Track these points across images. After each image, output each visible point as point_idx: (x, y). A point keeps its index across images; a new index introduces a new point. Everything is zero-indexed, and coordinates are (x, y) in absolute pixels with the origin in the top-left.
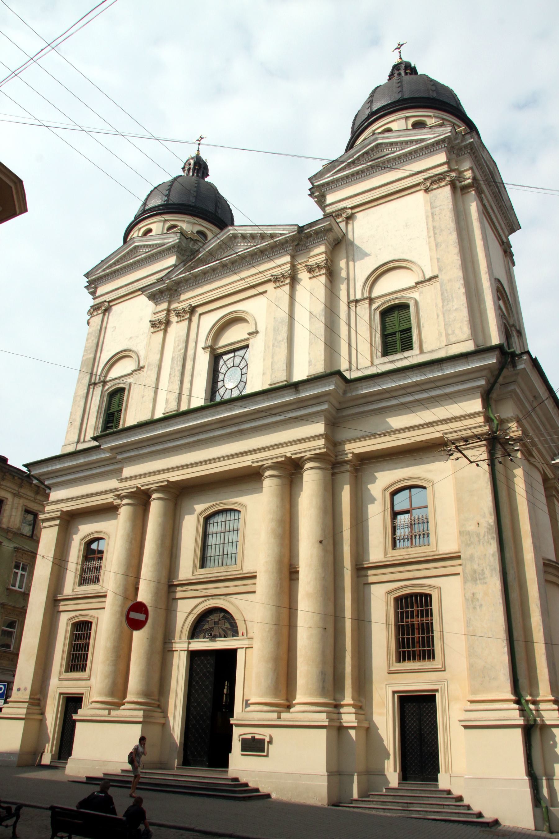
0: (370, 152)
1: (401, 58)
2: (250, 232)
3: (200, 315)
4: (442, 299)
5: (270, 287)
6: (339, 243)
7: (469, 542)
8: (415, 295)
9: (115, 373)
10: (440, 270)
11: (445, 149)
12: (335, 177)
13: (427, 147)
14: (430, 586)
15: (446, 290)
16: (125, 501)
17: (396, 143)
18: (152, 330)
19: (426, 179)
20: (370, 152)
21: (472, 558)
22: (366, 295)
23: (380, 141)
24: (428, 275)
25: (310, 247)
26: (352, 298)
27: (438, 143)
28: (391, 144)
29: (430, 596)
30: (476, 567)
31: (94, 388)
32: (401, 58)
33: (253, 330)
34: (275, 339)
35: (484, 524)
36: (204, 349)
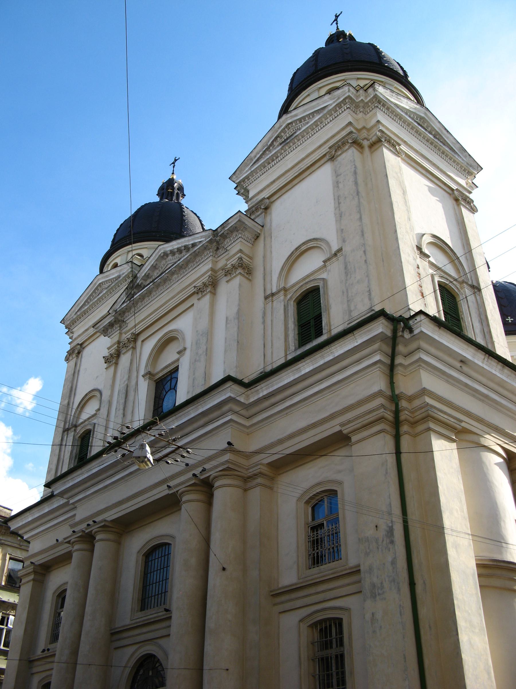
0: (282, 134)
1: (338, 29)
2: (176, 247)
3: (143, 341)
4: (346, 273)
5: (194, 300)
6: (258, 237)
7: (368, 551)
8: (324, 276)
9: (84, 416)
10: (344, 241)
11: (348, 110)
12: (252, 170)
13: (330, 113)
15: (349, 262)
16: (76, 547)
17: (304, 118)
18: (105, 365)
19: (330, 148)
20: (282, 134)
21: (370, 570)
22: (282, 286)
23: (289, 121)
25: (228, 249)
26: (268, 292)
27: (339, 105)
28: (300, 120)
30: (375, 580)
31: (68, 434)
32: (338, 29)
33: (181, 348)
34: (197, 353)
35: (383, 527)
36: (143, 376)
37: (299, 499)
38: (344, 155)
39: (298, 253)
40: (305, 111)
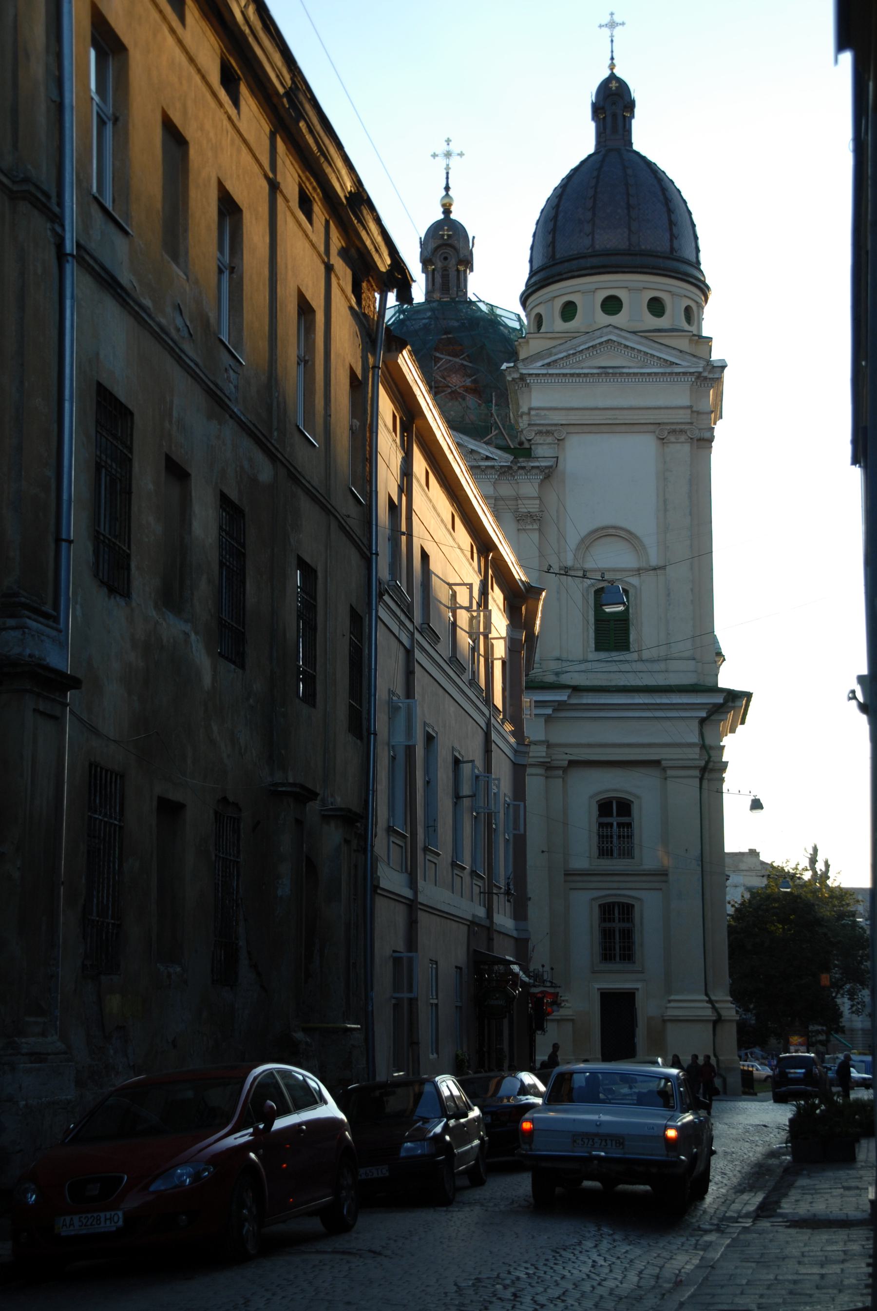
8: (634, 581)
12: (550, 371)
14: (633, 897)
17: (633, 349)
23: (614, 338)
24: (654, 561)
27: (685, 374)
29: (633, 906)
37: (591, 797)
38: (678, 446)
39: (604, 532)
40: (640, 343)
